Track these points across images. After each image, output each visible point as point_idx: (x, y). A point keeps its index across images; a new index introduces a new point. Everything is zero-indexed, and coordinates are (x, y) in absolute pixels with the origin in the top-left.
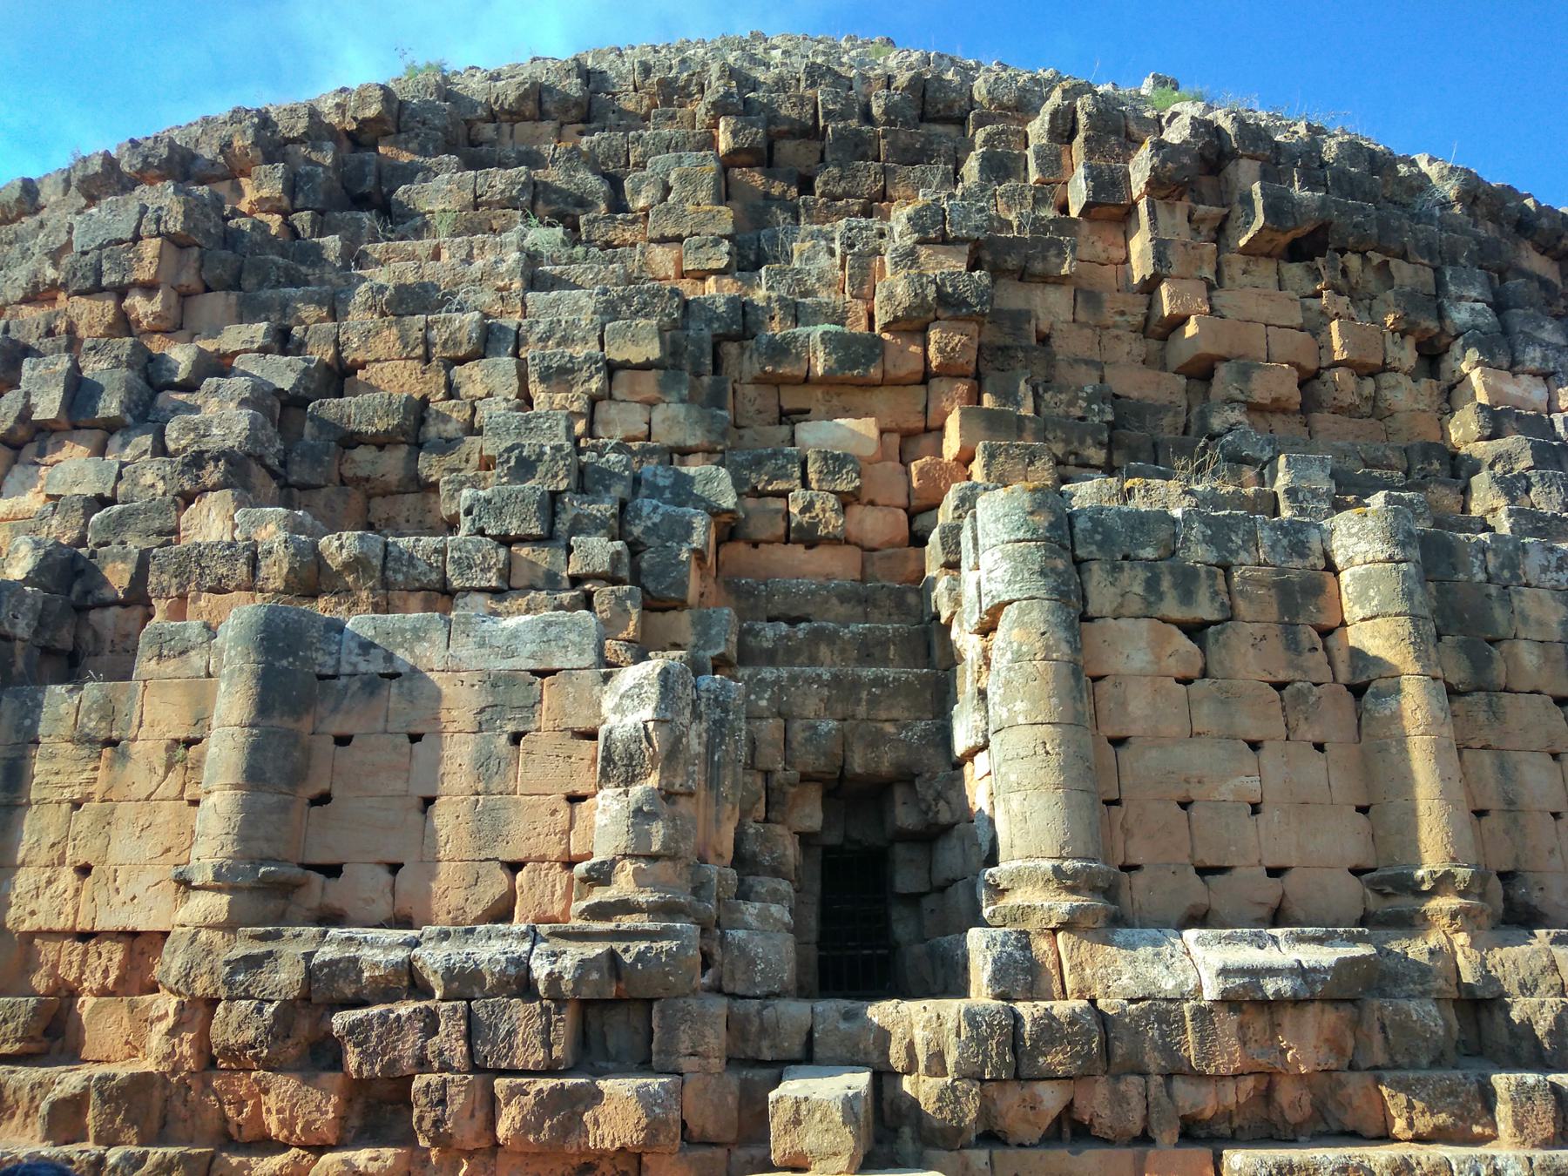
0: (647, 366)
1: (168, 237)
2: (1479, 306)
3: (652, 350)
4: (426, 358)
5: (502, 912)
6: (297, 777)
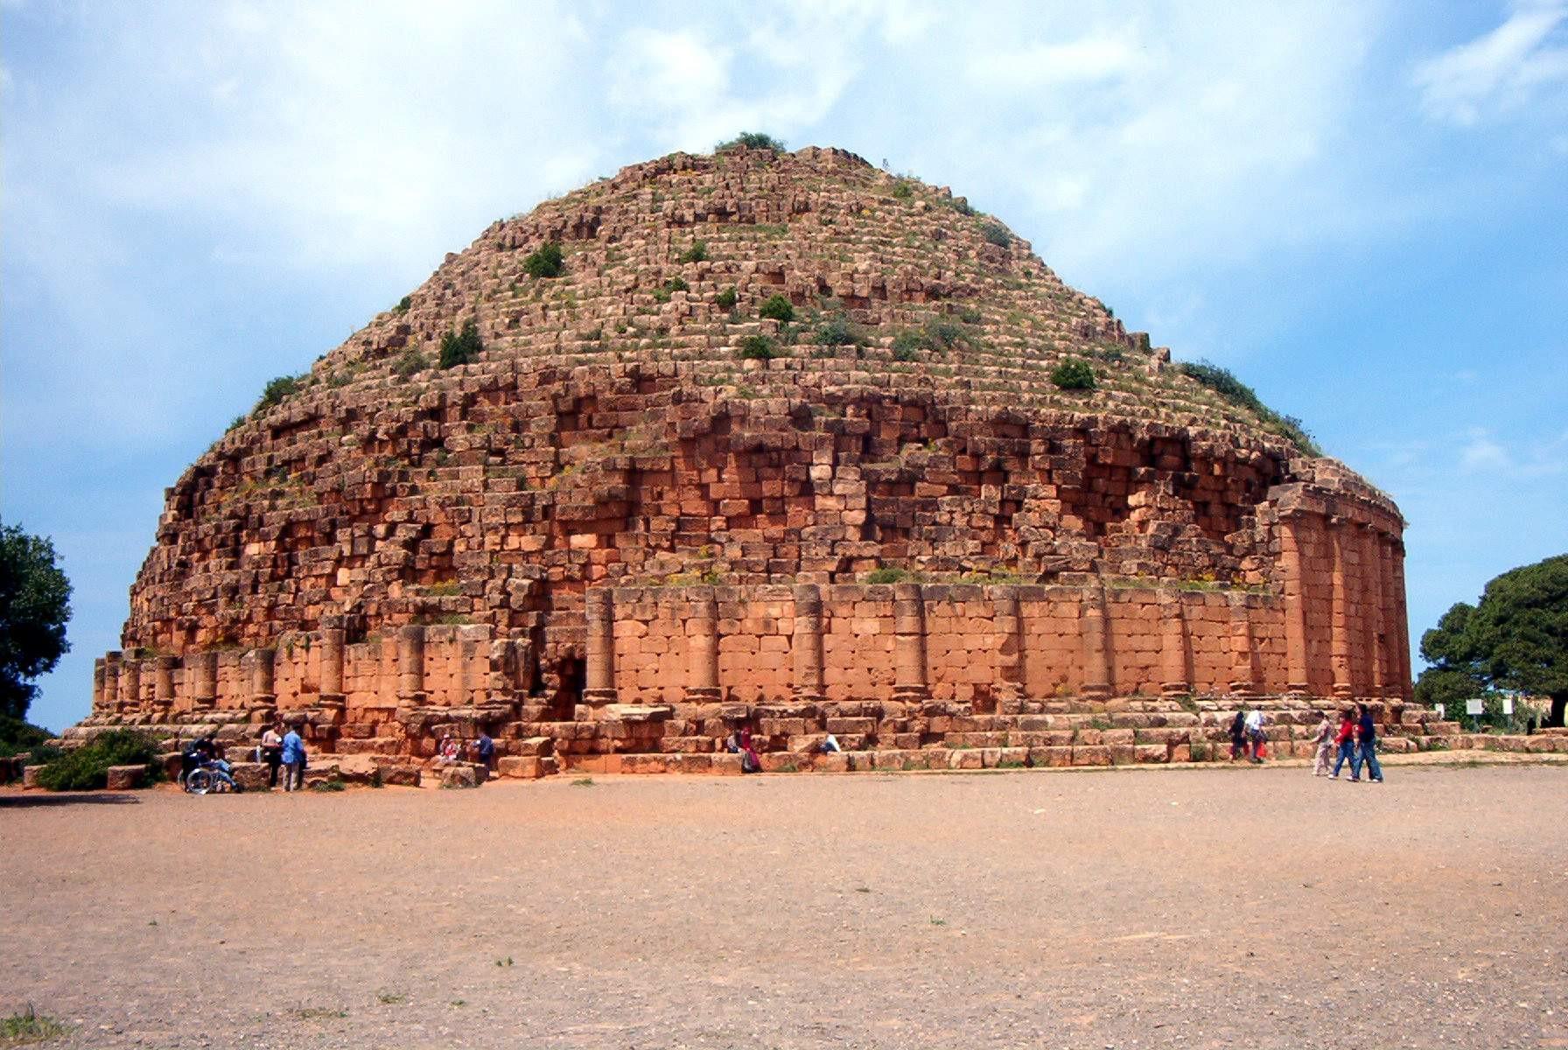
1: (374, 483)
2: (824, 467)
5: (471, 701)
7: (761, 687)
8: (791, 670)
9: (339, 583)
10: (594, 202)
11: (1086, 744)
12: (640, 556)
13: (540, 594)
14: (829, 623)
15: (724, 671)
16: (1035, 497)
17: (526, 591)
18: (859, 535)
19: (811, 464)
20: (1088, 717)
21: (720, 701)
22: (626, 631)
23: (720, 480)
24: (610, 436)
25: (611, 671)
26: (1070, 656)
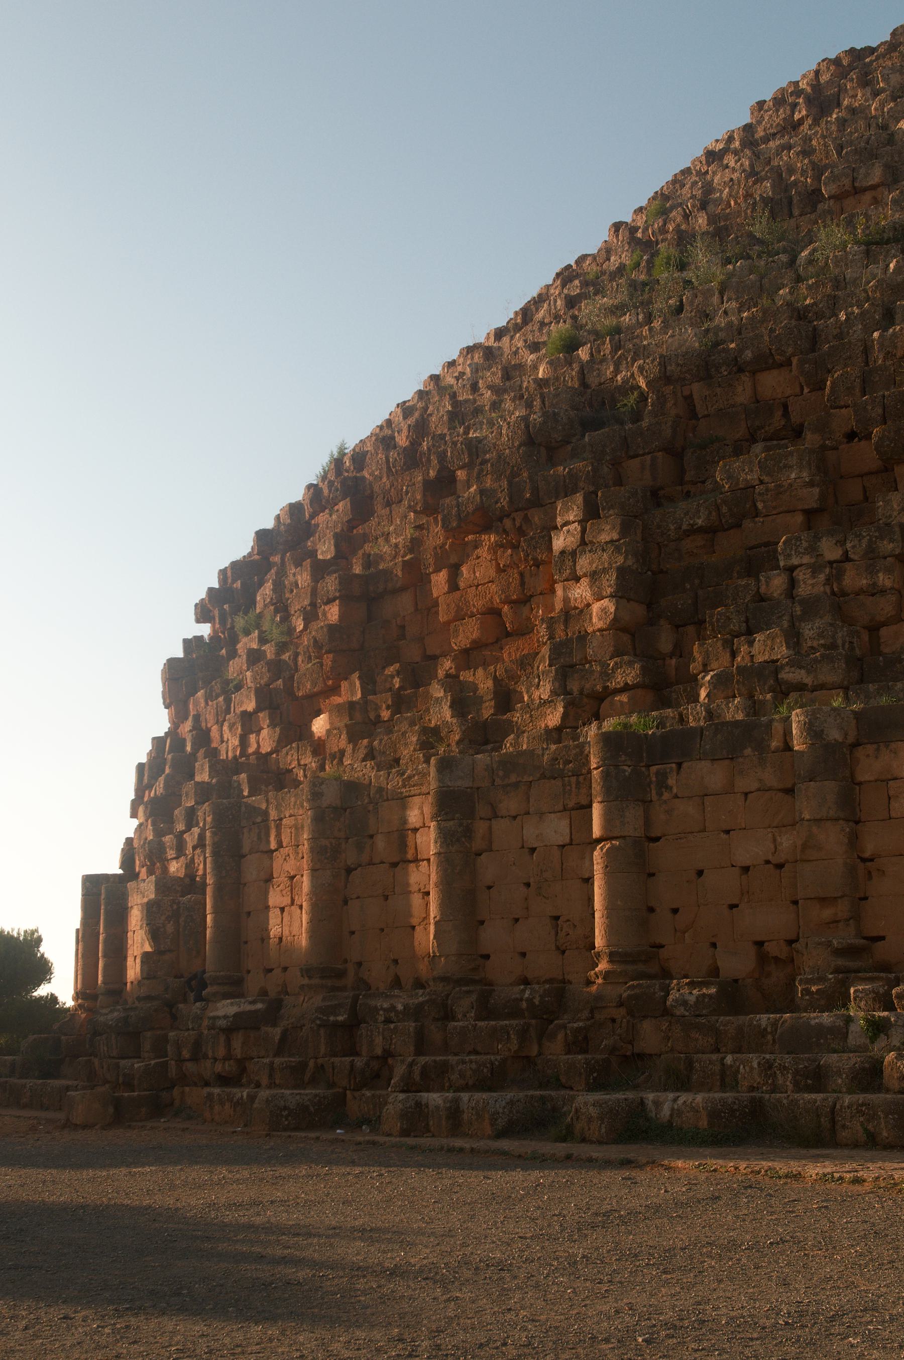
7: (396, 962)
14: (490, 828)
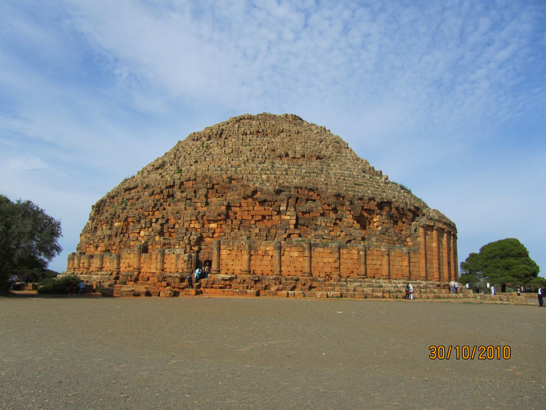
0: (194, 220)
3: (195, 219)
4: (175, 219)
5: (177, 272)
6: (164, 261)
7: (263, 271)
8: (272, 266)
9: (141, 235)
10: (221, 127)
11: (358, 292)
12: (229, 231)
13: (200, 240)
14: (284, 253)
15: (252, 265)
16: (346, 218)
17: (195, 240)
18: (293, 227)
19: (280, 206)
20: (359, 284)
21: (250, 274)
22: (224, 252)
23: (253, 210)
24: (222, 196)
25: (219, 264)
26: (354, 265)
